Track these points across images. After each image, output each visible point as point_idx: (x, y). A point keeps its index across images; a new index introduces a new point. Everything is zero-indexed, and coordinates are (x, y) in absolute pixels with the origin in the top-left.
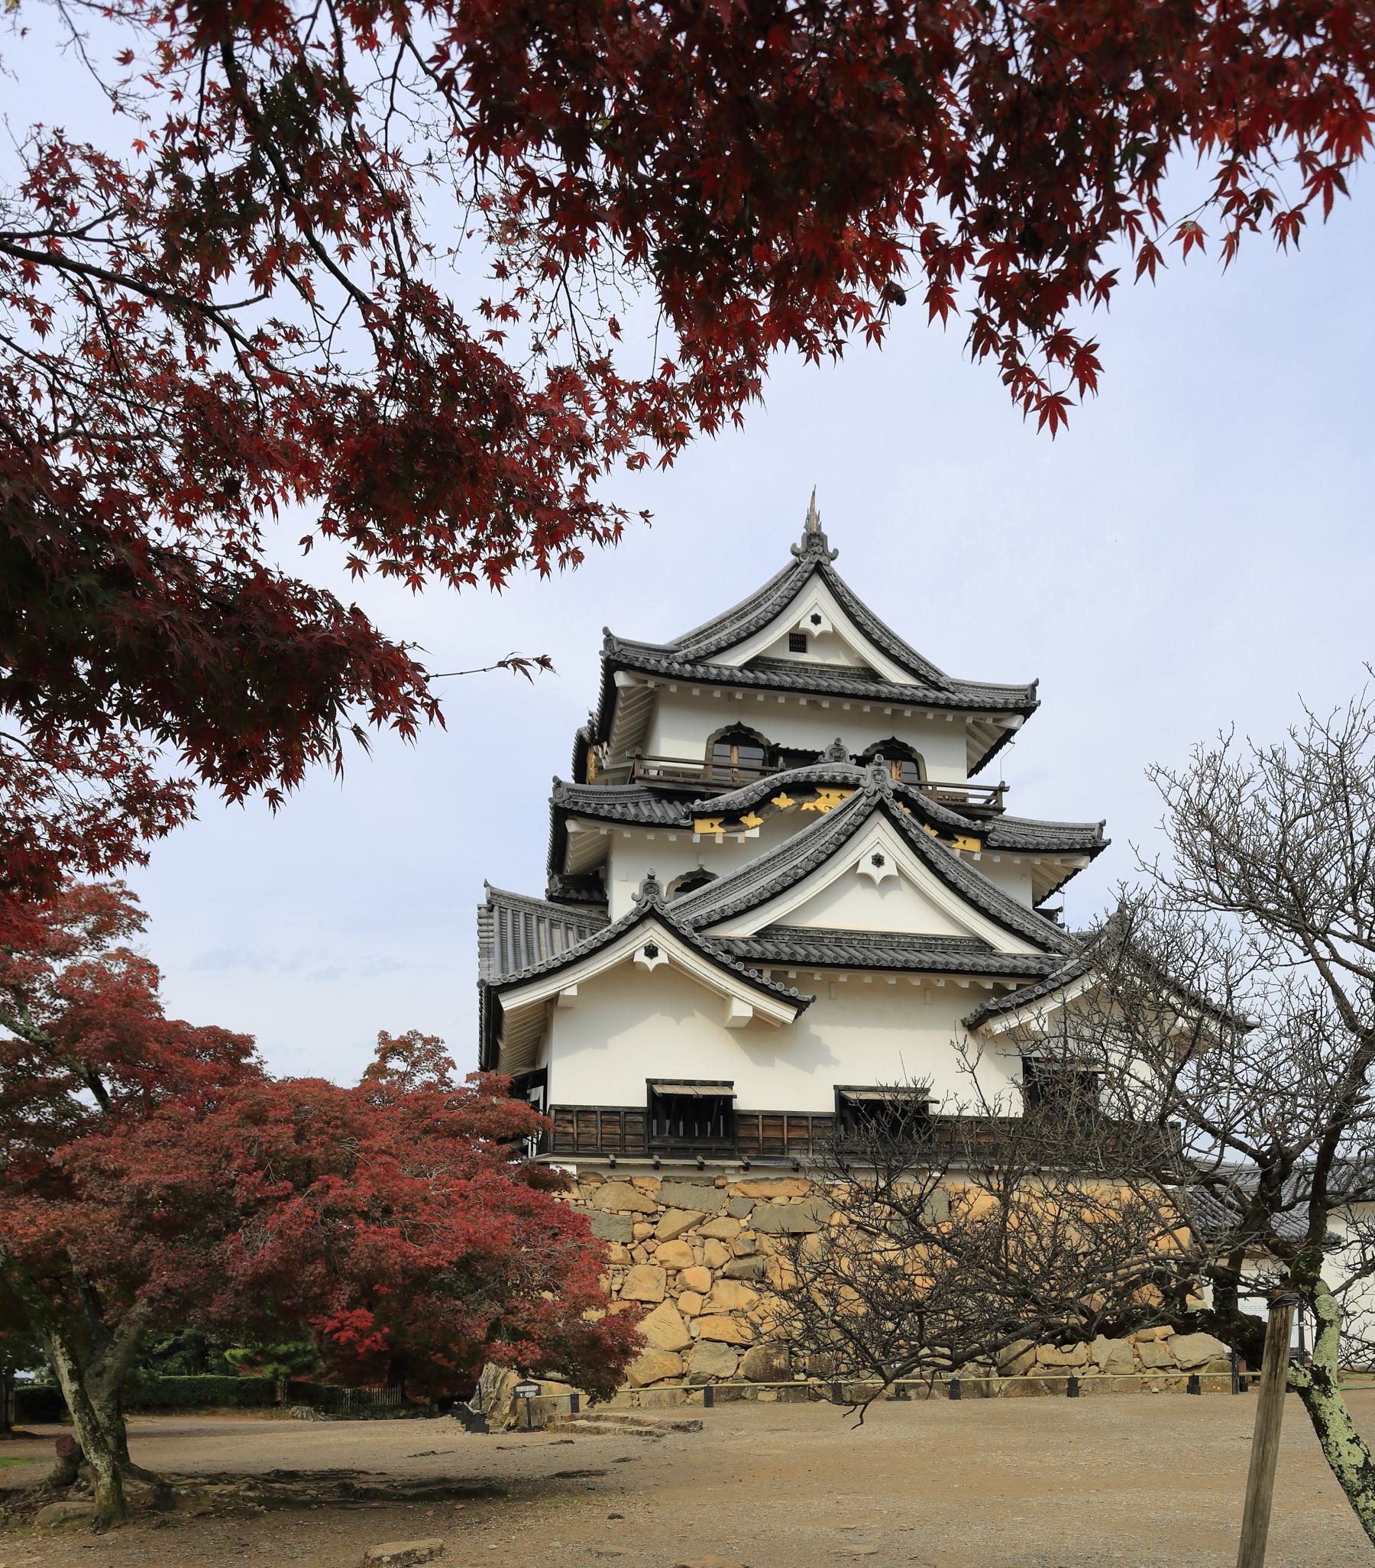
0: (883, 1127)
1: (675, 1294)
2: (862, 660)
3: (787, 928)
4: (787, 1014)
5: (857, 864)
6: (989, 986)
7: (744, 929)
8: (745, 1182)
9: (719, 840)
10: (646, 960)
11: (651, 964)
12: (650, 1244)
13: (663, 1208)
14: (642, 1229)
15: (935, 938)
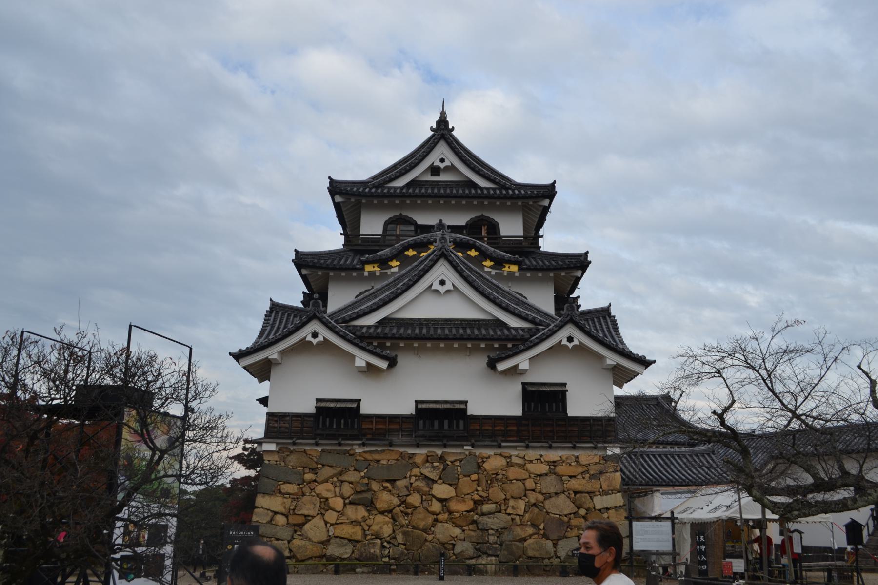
0: (441, 422)
1: (323, 512)
3: (394, 319)
4: (383, 364)
5: (431, 285)
7: (371, 320)
8: (365, 452)
9: (378, 274)
11: (315, 341)
12: (313, 485)
14: (309, 476)
15: (474, 320)
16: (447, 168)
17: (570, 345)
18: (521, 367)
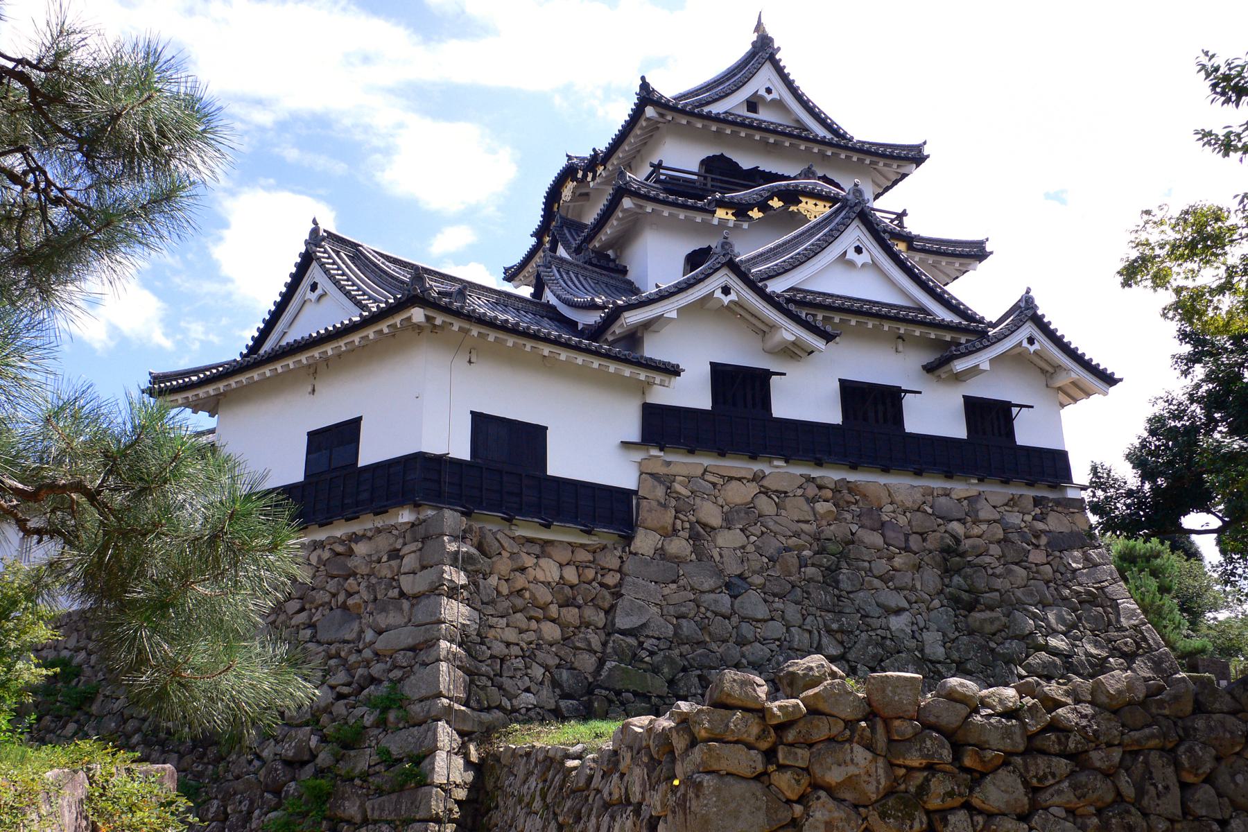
2: (798, 121)
6: (948, 338)
10: (722, 297)
11: (726, 300)
16: (772, 100)
17: (1032, 349)
18: (982, 367)
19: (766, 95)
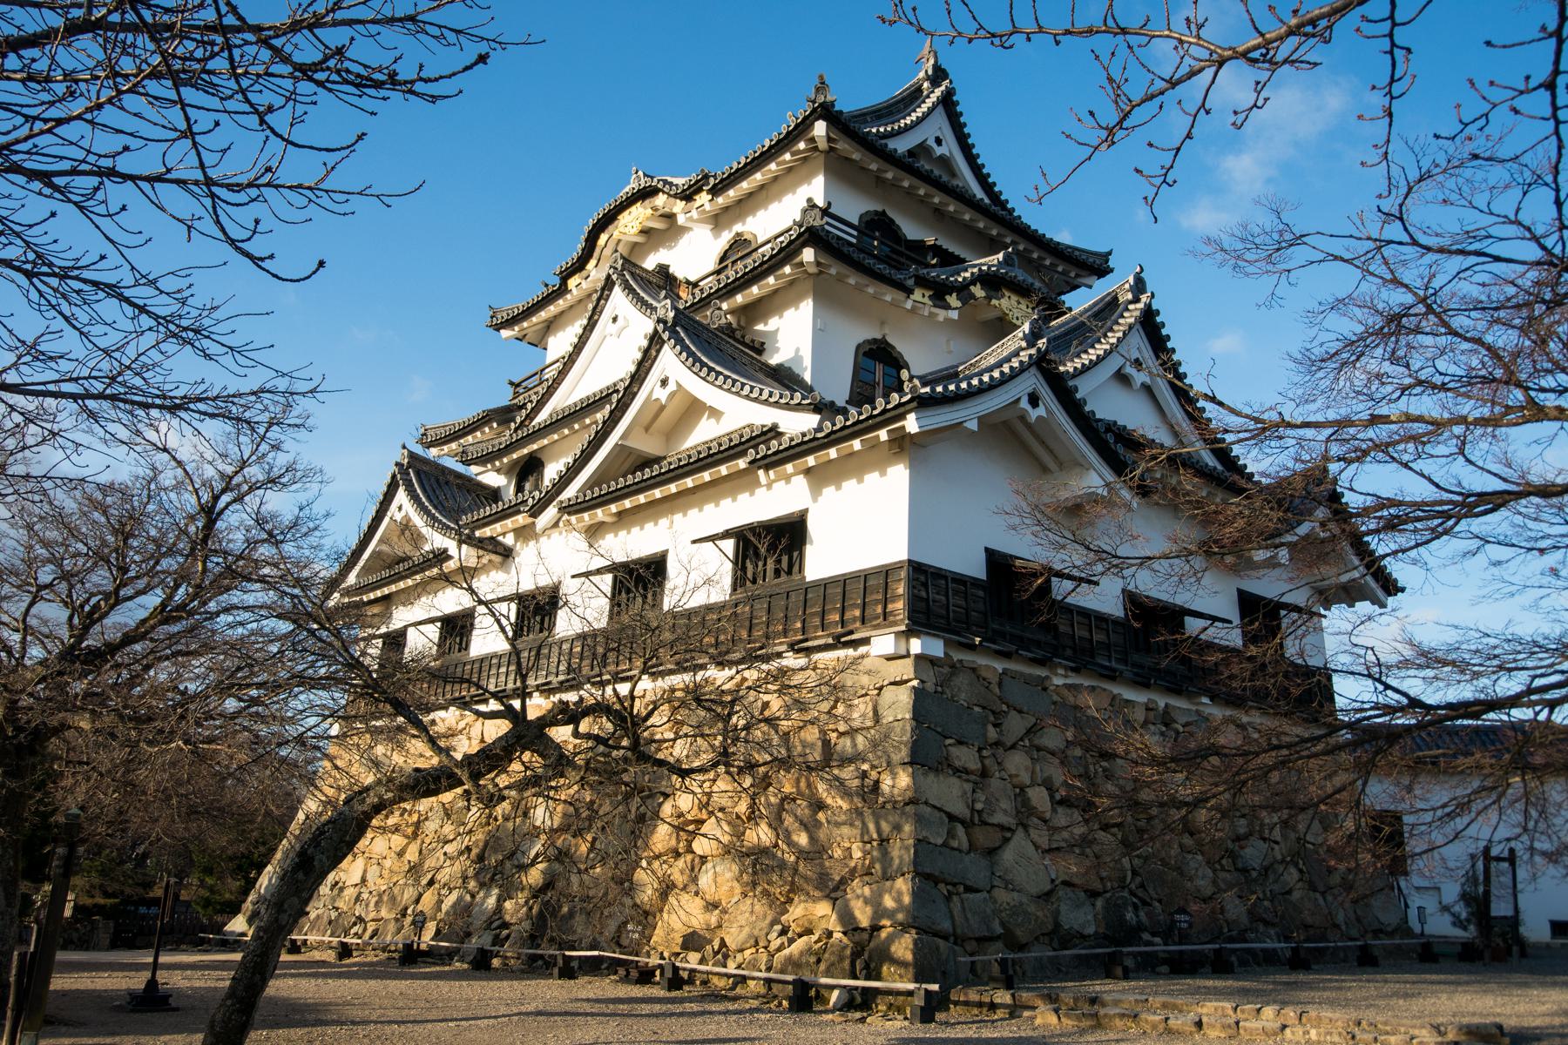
10: (1028, 407)
13: (1004, 708)
19: (934, 145)
